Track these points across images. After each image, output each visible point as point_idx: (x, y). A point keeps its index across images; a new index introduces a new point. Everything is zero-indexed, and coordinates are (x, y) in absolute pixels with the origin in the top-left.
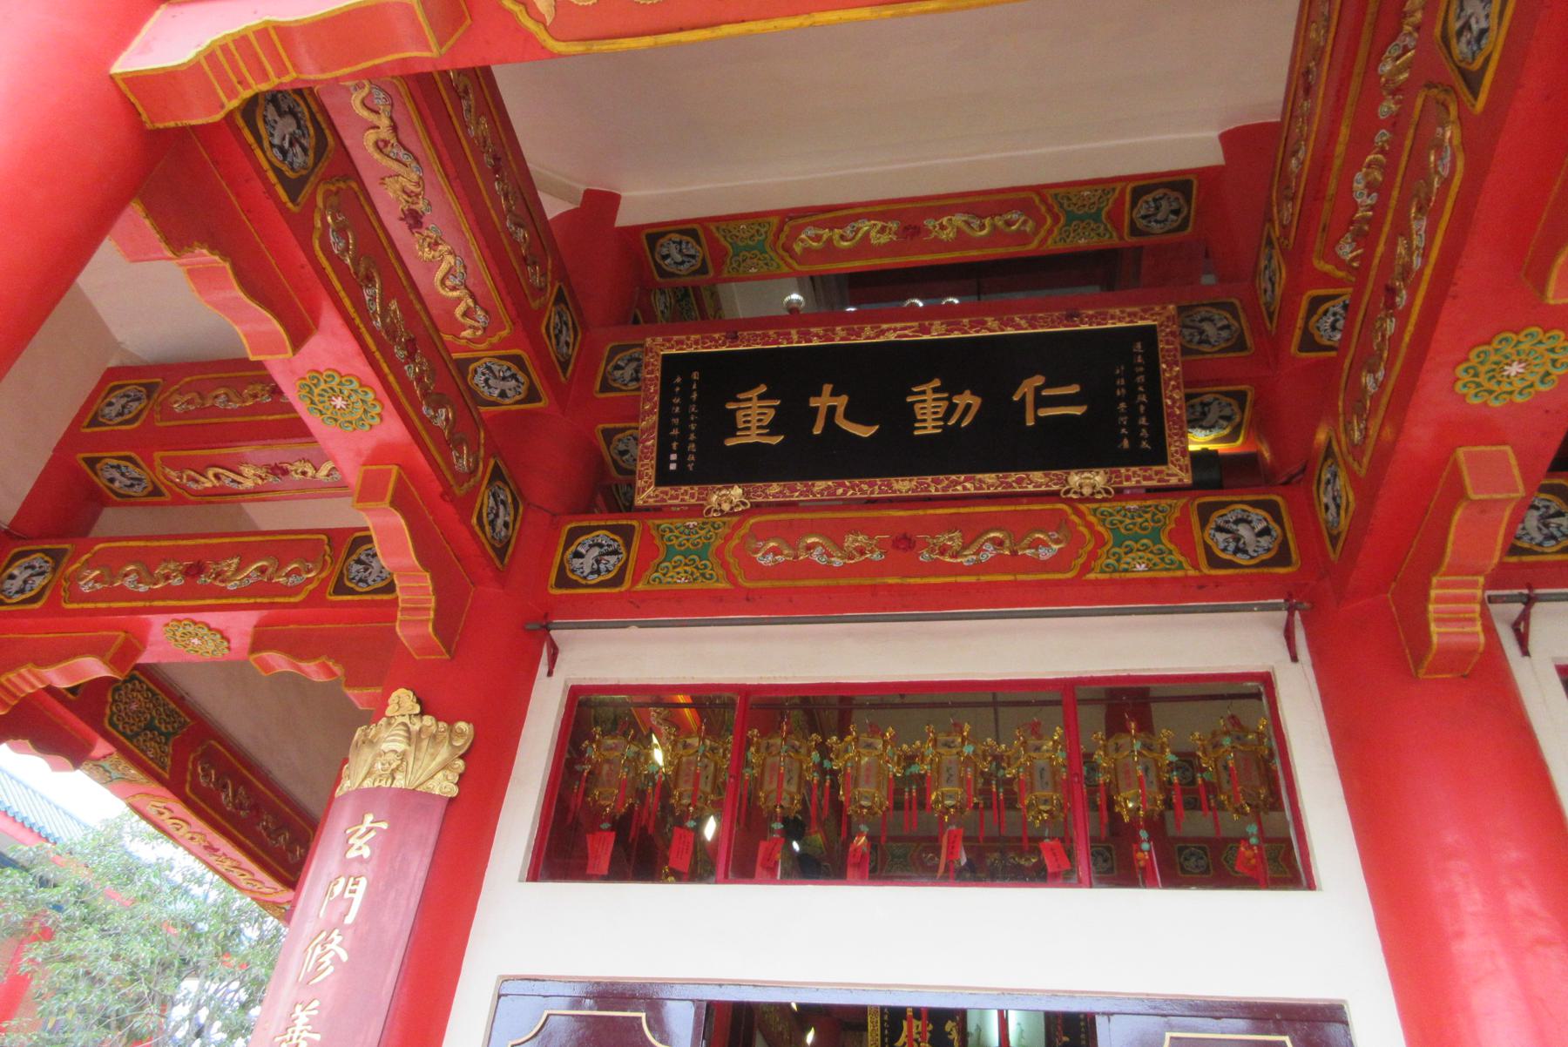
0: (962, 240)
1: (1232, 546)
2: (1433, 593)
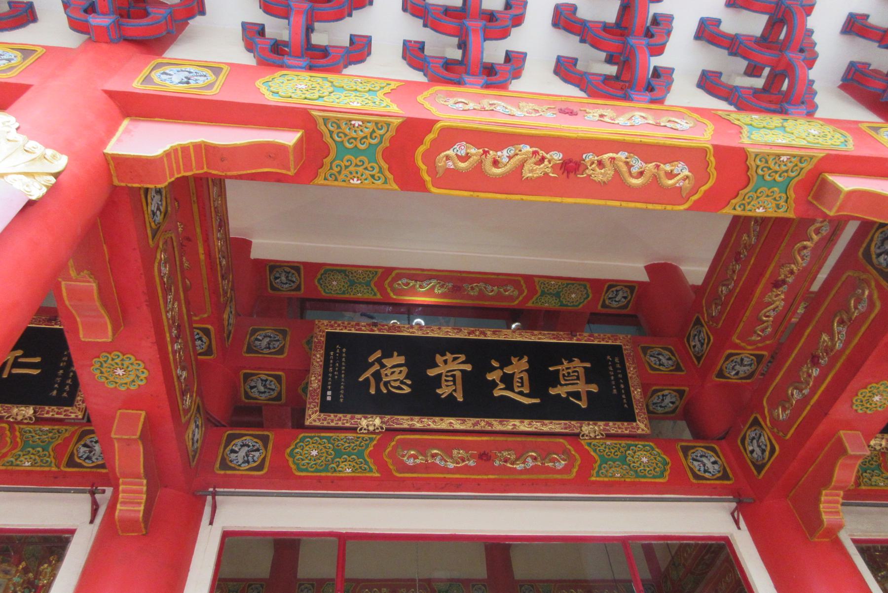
0: (482, 296)
1: (702, 469)
2: (823, 498)
